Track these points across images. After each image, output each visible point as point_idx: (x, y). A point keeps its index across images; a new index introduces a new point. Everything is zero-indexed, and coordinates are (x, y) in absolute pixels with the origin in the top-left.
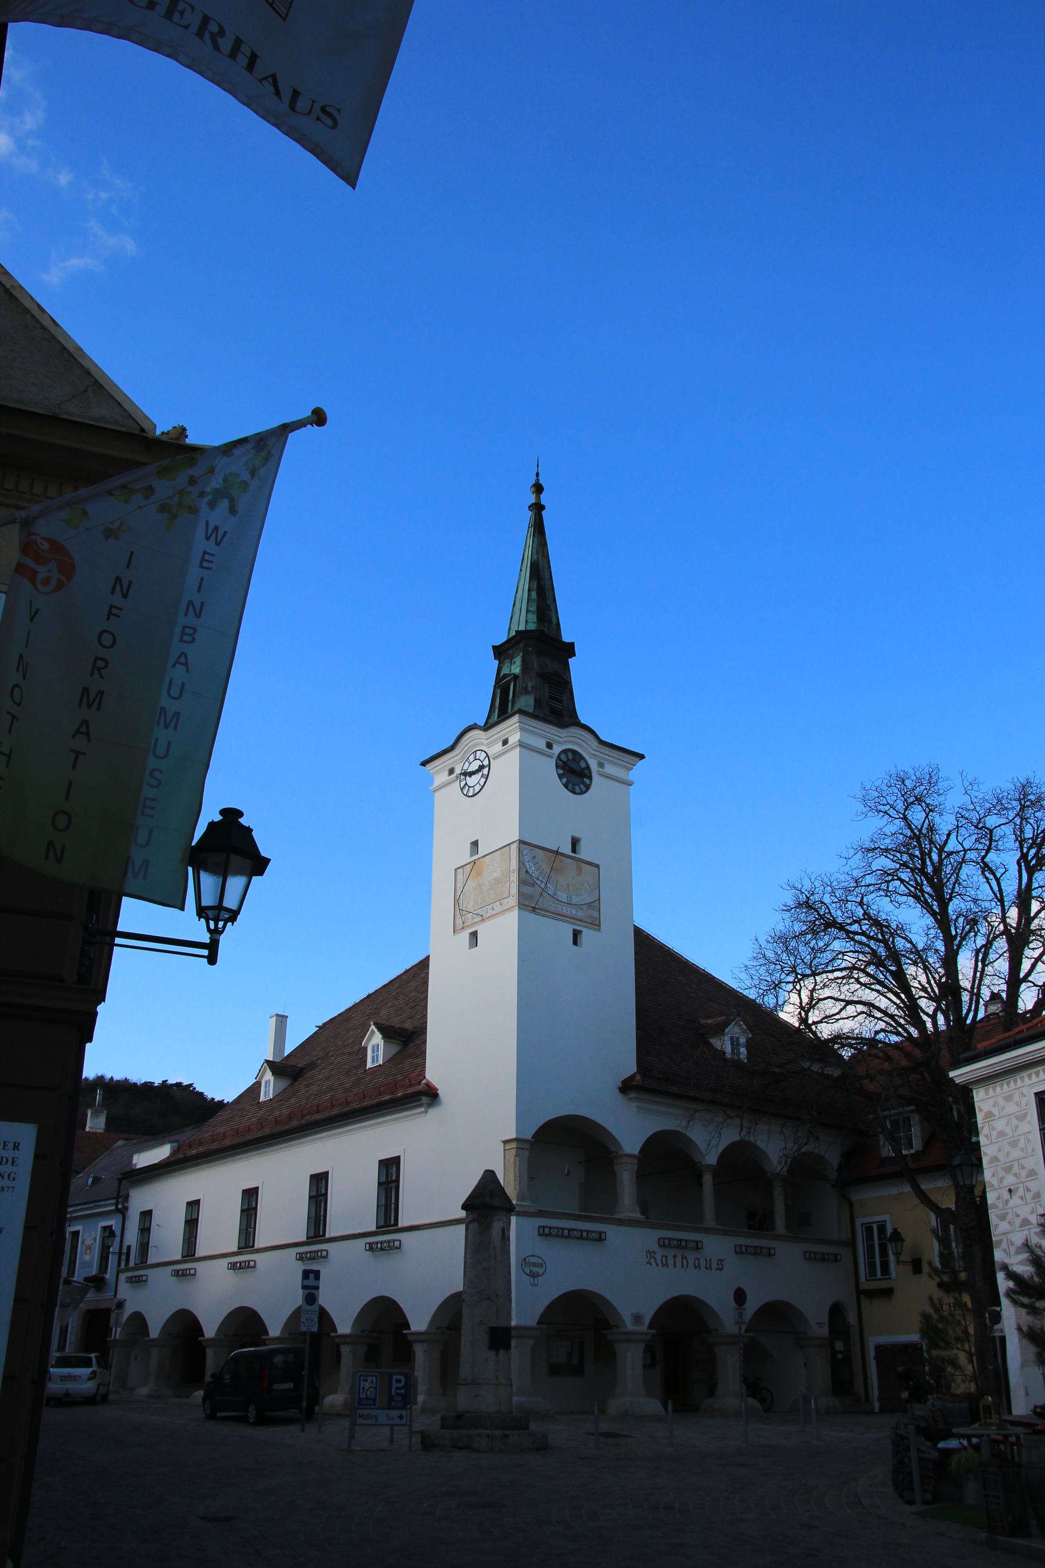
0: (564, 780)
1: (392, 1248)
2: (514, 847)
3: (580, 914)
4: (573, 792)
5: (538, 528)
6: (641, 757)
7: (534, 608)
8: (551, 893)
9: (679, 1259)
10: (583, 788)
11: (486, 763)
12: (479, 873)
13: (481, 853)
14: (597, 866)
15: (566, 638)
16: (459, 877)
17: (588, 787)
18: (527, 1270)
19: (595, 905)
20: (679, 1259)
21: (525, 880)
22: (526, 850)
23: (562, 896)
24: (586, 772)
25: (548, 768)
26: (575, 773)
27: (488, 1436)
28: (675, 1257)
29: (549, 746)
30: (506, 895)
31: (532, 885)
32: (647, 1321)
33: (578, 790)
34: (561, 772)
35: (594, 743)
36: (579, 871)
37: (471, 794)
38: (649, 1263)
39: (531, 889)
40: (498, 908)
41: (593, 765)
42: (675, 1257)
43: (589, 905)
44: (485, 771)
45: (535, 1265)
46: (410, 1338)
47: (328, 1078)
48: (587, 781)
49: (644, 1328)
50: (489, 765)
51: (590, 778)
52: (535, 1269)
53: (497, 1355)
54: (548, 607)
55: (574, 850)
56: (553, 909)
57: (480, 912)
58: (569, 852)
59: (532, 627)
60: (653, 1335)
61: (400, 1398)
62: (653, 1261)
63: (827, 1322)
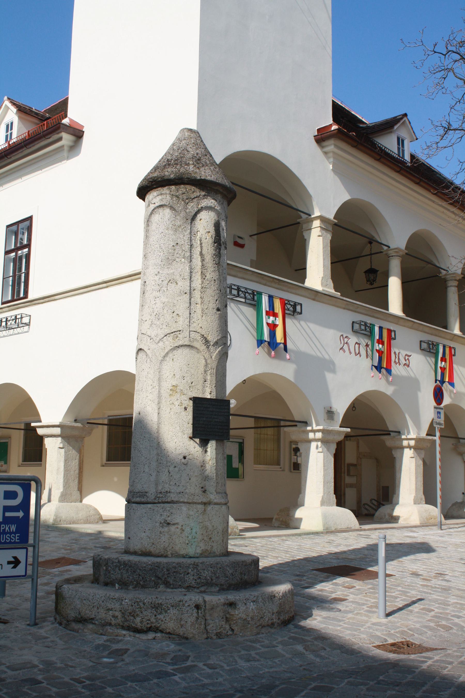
1: (19, 323)
27: (197, 607)
46: (40, 432)
61: (13, 528)
62: (346, 347)
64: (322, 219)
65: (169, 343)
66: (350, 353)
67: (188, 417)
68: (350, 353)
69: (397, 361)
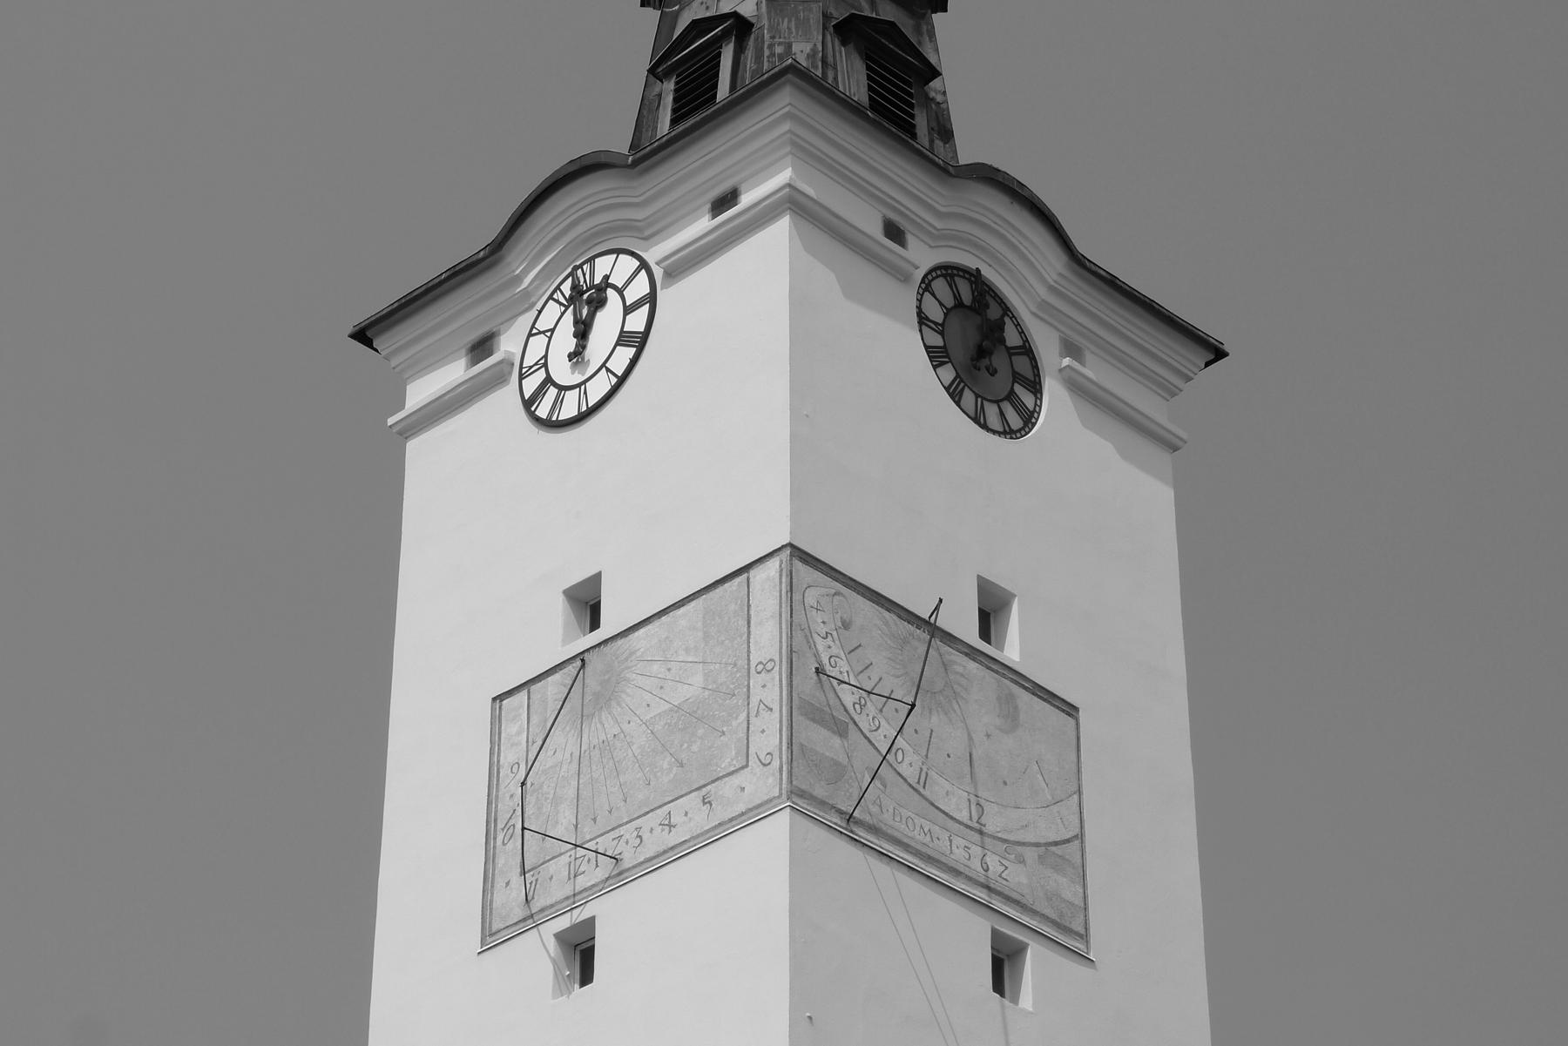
2: (768, 578)
3: (1017, 878)
4: (979, 419)
8: (909, 772)
10: (1015, 421)
12: (606, 698)
13: (611, 622)
14: (1070, 710)
16: (514, 729)
17: (1029, 419)
19: (1065, 853)
21: (814, 705)
22: (817, 588)
29: (894, 233)
30: (727, 762)
33: (993, 420)
34: (937, 340)
35: (1052, 261)
36: (1011, 718)
39: (836, 741)
40: (691, 817)
48: (1028, 400)
50: (651, 299)
51: (1036, 388)
55: (985, 634)
56: (917, 837)
57: (603, 844)
58: (968, 630)
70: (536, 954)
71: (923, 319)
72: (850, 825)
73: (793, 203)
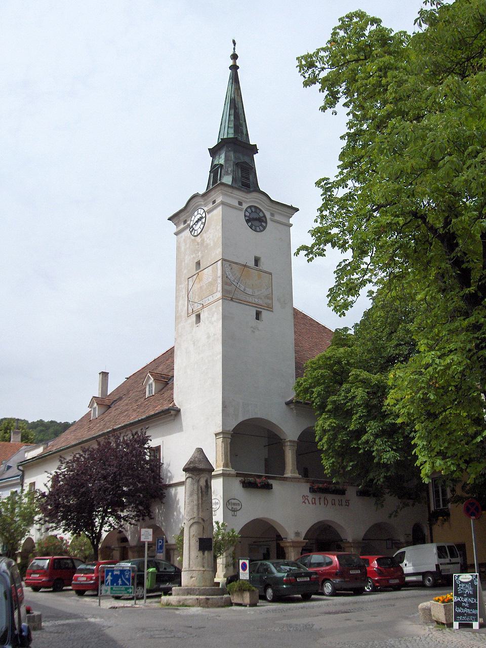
0: (250, 224)
2: (220, 262)
3: (260, 302)
4: (255, 231)
5: (235, 79)
6: (297, 210)
7: (232, 125)
9: (322, 499)
10: (262, 229)
11: (204, 215)
12: (200, 280)
13: (202, 267)
14: (271, 274)
15: (252, 143)
16: (191, 283)
17: (264, 228)
18: (230, 507)
20: (322, 499)
21: (226, 281)
22: (227, 264)
23: (249, 291)
24: (264, 219)
25: (240, 217)
26: (256, 220)
28: (320, 498)
29: (240, 203)
31: (230, 285)
32: (303, 535)
33: (258, 229)
37: (196, 234)
38: (304, 502)
41: (268, 216)
42: (320, 498)
43: (267, 297)
44: (203, 220)
45: (234, 504)
47: (127, 405)
49: (301, 539)
51: (266, 222)
52: (234, 507)
53: (204, 554)
54: (241, 125)
56: (243, 298)
57: (201, 302)
59: (231, 136)
60: (307, 543)
62: (306, 501)
63: (411, 533)
64: (290, 441)
65: (192, 521)
66: (309, 503)
67: (198, 544)
68: (309, 503)
69: (340, 503)
70: (193, 318)
71: (245, 216)
72: (232, 299)
73: (223, 203)
